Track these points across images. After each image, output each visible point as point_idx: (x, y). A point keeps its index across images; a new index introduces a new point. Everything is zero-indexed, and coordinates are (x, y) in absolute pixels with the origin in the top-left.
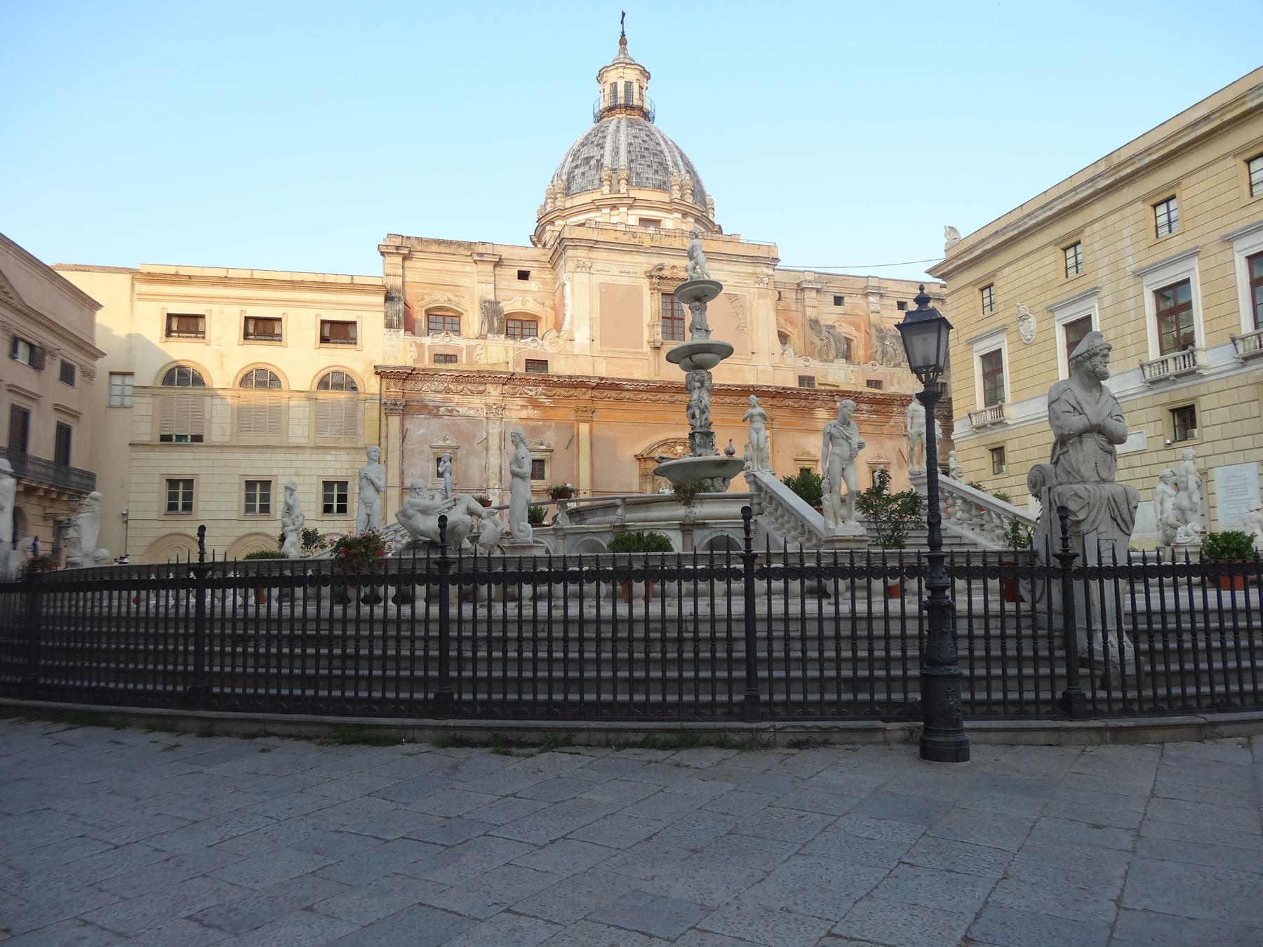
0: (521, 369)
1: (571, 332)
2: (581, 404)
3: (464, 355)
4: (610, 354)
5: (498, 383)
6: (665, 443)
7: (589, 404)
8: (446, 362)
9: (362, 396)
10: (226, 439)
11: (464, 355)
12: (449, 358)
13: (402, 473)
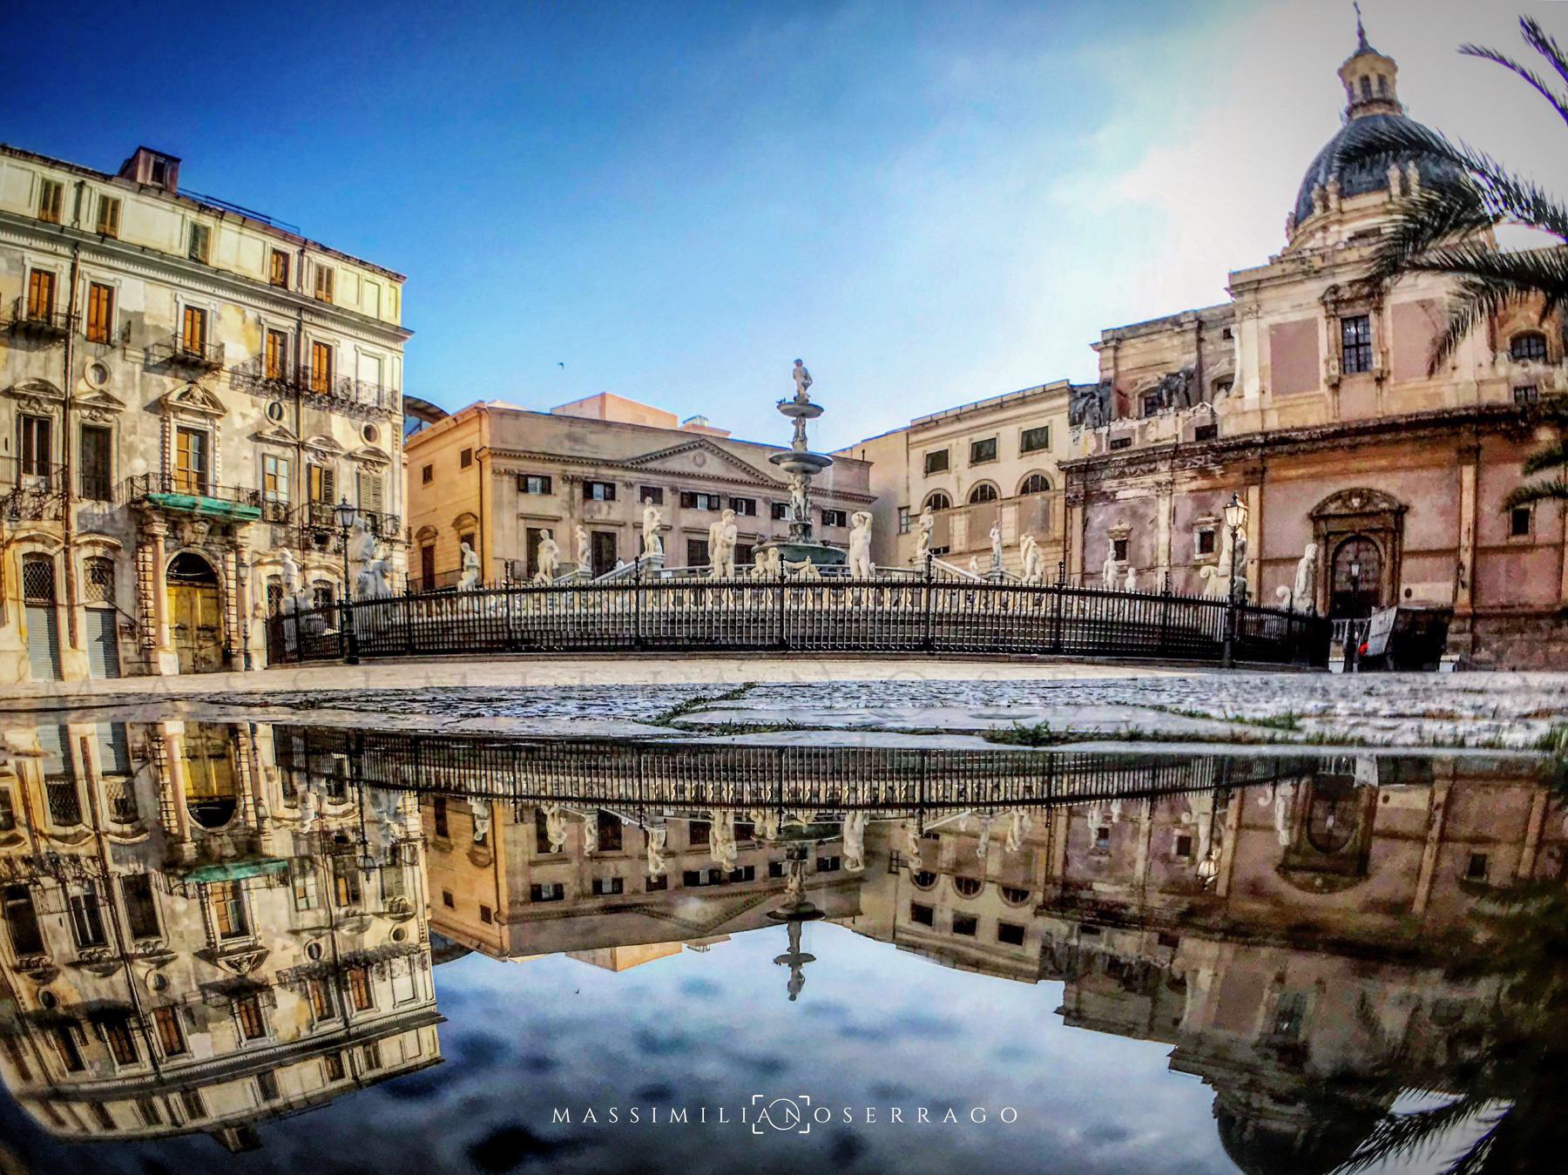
0: (1192, 438)
1: (1241, 388)
2: (1250, 466)
3: (1137, 436)
4: (1282, 404)
5: (1165, 459)
6: (1337, 496)
7: (1259, 466)
8: (1122, 446)
9: (1052, 494)
10: (962, 548)
11: (1137, 436)
12: (1125, 443)
13: (1083, 559)
